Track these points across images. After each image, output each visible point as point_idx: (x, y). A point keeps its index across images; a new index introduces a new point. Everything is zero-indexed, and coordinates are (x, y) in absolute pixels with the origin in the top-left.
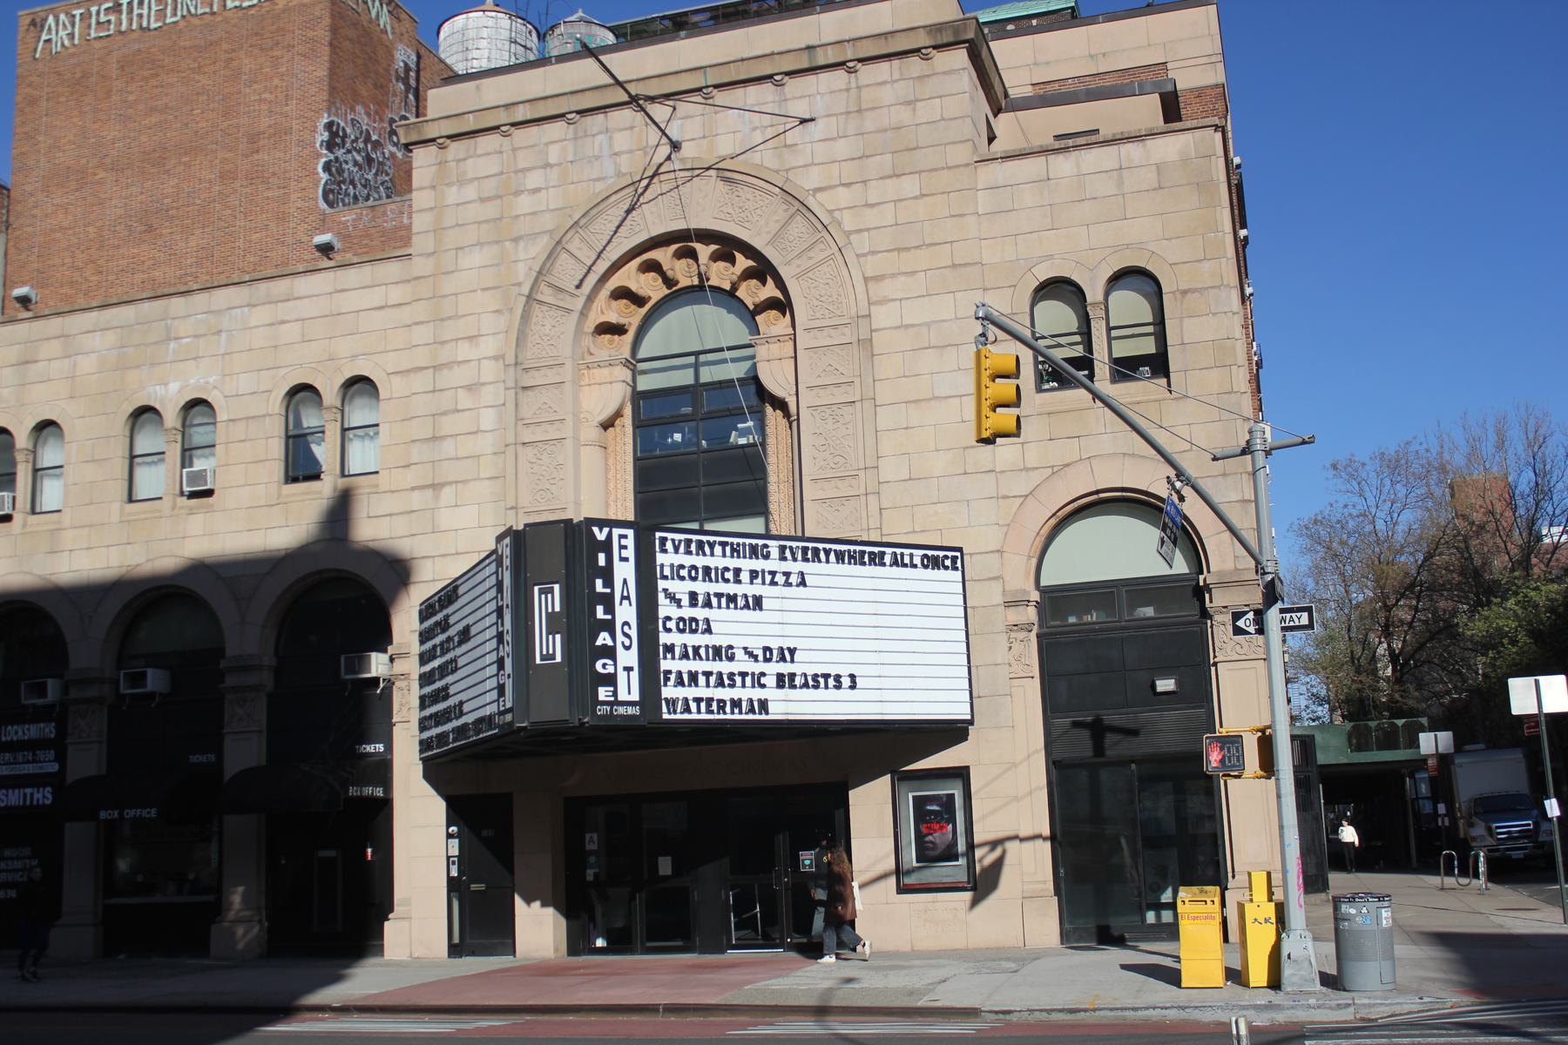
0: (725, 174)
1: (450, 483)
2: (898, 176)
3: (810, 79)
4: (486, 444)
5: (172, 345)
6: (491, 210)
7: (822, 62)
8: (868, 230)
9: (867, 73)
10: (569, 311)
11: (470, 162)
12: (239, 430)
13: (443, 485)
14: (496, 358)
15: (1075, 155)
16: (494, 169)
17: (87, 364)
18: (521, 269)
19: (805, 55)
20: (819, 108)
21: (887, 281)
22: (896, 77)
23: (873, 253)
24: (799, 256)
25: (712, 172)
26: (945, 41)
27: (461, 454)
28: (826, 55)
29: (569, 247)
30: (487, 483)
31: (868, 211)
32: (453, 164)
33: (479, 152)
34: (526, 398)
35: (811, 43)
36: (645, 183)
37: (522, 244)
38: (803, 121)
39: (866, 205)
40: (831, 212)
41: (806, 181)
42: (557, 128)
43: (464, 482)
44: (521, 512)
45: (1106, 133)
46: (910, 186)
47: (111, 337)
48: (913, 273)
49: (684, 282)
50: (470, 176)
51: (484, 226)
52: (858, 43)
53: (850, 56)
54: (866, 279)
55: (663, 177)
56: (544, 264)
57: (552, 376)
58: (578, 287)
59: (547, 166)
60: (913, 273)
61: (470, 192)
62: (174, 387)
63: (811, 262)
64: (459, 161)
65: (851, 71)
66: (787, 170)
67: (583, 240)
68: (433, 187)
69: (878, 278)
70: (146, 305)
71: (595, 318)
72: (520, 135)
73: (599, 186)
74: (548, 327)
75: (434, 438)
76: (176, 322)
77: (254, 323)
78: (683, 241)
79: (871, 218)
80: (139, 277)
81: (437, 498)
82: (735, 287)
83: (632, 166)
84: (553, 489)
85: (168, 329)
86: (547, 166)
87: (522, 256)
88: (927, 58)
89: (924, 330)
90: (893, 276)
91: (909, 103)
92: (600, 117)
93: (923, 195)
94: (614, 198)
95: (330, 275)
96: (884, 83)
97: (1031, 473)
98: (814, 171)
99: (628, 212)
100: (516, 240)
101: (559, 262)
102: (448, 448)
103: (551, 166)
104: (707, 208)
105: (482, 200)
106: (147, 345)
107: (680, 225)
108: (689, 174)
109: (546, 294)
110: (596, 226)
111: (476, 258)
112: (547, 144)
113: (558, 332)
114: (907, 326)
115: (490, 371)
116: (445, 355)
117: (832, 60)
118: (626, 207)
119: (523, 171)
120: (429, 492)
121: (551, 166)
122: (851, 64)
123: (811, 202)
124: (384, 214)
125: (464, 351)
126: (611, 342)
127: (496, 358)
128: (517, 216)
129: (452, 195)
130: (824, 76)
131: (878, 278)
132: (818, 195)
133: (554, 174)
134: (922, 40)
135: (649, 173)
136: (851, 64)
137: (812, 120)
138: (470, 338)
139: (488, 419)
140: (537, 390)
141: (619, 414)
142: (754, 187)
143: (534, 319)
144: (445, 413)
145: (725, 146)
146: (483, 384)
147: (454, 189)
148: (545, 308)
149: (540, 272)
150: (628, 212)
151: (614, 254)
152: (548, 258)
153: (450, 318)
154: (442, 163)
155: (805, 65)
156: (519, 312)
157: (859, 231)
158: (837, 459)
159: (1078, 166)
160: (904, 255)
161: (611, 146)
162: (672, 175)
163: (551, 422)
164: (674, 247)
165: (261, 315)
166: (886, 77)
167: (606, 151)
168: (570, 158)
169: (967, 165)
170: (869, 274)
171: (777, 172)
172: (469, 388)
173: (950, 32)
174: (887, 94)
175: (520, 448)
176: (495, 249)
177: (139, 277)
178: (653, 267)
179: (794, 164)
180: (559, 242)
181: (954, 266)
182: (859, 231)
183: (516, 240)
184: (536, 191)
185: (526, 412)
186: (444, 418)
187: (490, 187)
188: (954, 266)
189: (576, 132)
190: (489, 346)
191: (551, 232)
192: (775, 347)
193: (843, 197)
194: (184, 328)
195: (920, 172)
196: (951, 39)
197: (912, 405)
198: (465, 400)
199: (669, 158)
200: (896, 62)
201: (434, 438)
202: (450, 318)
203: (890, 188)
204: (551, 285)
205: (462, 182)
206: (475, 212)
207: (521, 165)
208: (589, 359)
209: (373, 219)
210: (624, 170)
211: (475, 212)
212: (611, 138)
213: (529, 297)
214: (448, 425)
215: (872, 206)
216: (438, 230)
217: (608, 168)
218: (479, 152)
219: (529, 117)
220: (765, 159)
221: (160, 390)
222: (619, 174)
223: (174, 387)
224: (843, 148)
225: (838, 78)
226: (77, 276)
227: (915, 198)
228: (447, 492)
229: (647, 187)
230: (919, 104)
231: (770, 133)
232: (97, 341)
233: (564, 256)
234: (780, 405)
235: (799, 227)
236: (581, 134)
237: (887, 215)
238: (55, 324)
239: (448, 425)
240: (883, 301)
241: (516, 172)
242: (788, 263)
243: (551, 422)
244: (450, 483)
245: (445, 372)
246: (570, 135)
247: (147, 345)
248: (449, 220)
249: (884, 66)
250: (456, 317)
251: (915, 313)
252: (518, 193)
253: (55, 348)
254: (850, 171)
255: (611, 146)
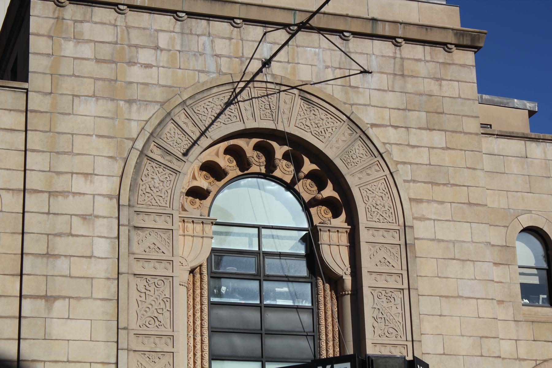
0: (305, 94)
1: (64, 298)
2: (431, 130)
3: (367, 43)
4: (101, 269)
6: (105, 71)
7: (380, 32)
8: (410, 164)
9: (409, 50)
10: (176, 172)
11: (86, 26)
13: (56, 298)
14: (110, 197)
15: (542, 145)
16: (111, 38)
18: (135, 128)
19: (370, 23)
20: (374, 64)
21: (425, 205)
22: (428, 58)
23: (414, 181)
24: (361, 171)
25: (295, 91)
26: (465, 43)
27: (74, 273)
28: (384, 29)
29: (176, 119)
30: (99, 302)
31: (410, 150)
32: (71, 23)
33: (95, 19)
34: (136, 236)
35: (376, 16)
36: (242, 85)
37: (135, 107)
38: (365, 72)
39: (408, 145)
40: (384, 144)
41: (366, 117)
42: (166, 21)
43: (78, 298)
44: (132, 333)
45: (496, 128)
46: (438, 139)
48: (442, 203)
49: (254, 169)
50: (86, 37)
51: (99, 83)
52: (407, 27)
53: (400, 34)
54: (411, 200)
55: (256, 84)
56: (155, 129)
57: (161, 223)
58: (185, 154)
59: (157, 48)
60: (442, 203)
61: (87, 51)
63: (370, 178)
64: (75, 21)
65: (397, 45)
66: (352, 105)
67: (188, 116)
68: (51, 37)
69: (419, 201)
71: (186, 183)
72: (134, 18)
73: (203, 78)
74: (157, 180)
75: (47, 255)
78: (265, 138)
79: (411, 155)
81: (50, 309)
82: (294, 181)
83: (231, 68)
84: (160, 317)
86: (157, 48)
87: (134, 116)
88: (449, 51)
89: (451, 245)
90: (428, 201)
91: (437, 79)
92: (204, 23)
93: (448, 148)
94: (215, 90)
96: (419, 60)
97: (522, 362)
98: (372, 111)
99: (228, 104)
100: (130, 102)
101: (167, 129)
102: (62, 266)
103: (162, 50)
104: (294, 119)
105: (98, 61)
107: (270, 125)
108: (278, 87)
109: (157, 154)
110: (200, 108)
111: (90, 108)
112: (157, 31)
113: (168, 186)
114: (439, 241)
115: (105, 207)
116: (60, 183)
117: (387, 33)
118: (226, 100)
119: (136, 46)
120: (41, 303)
121: (162, 50)
122: (399, 40)
123: (371, 132)
125: (79, 184)
126: (192, 203)
127: (110, 197)
128: (131, 83)
129: (69, 49)
130: (377, 43)
131: (419, 201)
132: (374, 129)
133: (164, 57)
134: (450, 38)
135: (247, 78)
136: (399, 40)
137: (371, 73)
138: (86, 175)
139: (102, 247)
140: (147, 232)
141: (201, 266)
142: (327, 111)
143: (146, 172)
144: (60, 235)
145: (305, 74)
146: (97, 217)
147: (71, 44)
148: (154, 165)
149: (151, 134)
150: (228, 104)
151: (216, 133)
152: (159, 124)
153: (65, 153)
154: (59, 19)
155: (369, 31)
156: (132, 162)
157: (404, 163)
158: (391, 330)
159: (545, 153)
160: (435, 187)
161: (213, 48)
162: (264, 85)
163: (160, 261)
164: (255, 141)
166: (421, 56)
167: (208, 51)
168: (178, 47)
169: (477, 134)
170: (413, 196)
171: (345, 103)
172: (84, 217)
173: (469, 38)
174: (422, 69)
175: (131, 278)
176: (110, 105)
178: (269, 153)
179: (356, 101)
180: (169, 114)
181: (470, 204)
182: (404, 163)
183: (130, 102)
184: (148, 66)
185: (137, 249)
186: (58, 239)
187: (106, 51)
188: (470, 204)
189: (182, 28)
190: (106, 185)
191: (162, 104)
192: (334, 235)
193: (392, 135)
195: (446, 131)
196: (469, 43)
197: (444, 299)
198: (78, 227)
199: (260, 71)
200: (428, 48)
201: (47, 255)
202: (65, 153)
203: (426, 137)
204: (160, 147)
205: (78, 40)
206: (89, 67)
207: (134, 42)
208: (184, 214)
210: (224, 70)
211: (89, 67)
212: (212, 41)
213: (142, 152)
214: (62, 245)
215: (414, 147)
216: (55, 75)
217: (211, 65)
218: (95, 19)
219: (146, 5)
220: (334, 91)
222: (220, 72)
224: (392, 99)
225: (386, 47)
227: (442, 149)
228: (59, 305)
229: (243, 89)
230: (444, 83)
231: (339, 73)
233: (171, 126)
234: (335, 282)
235: (359, 148)
236: (188, 31)
237: (423, 157)
239: (62, 245)
240: (422, 219)
241: (130, 46)
242: (353, 175)
243: (160, 261)
244: (64, 298)
245: (60, 198)
246: (177, 29)
248: (66, 68)
249: (419, 48)
250: (71, 153)
251: (446, 232)
252: (131, 63)
254: (396, 117)
255: (213, 48)
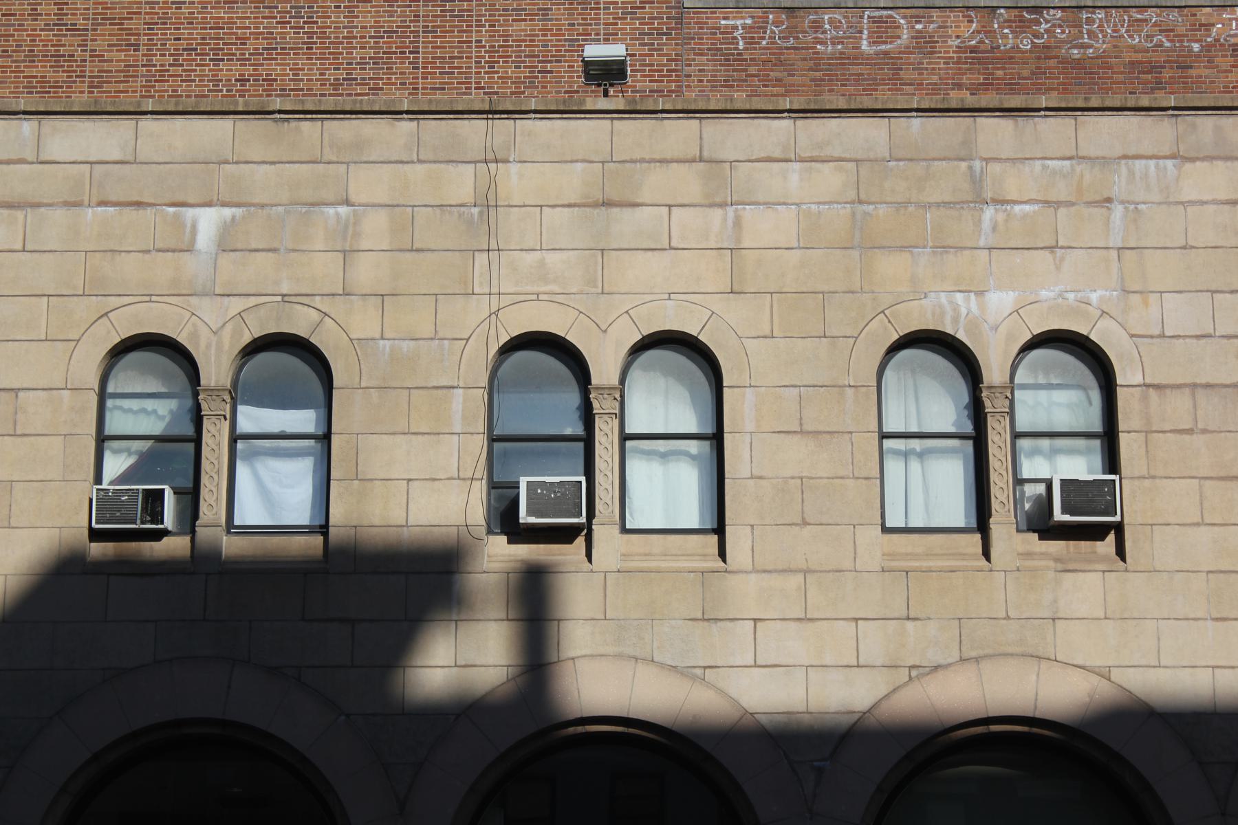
5: (989, 213)
12: (1178, 408)
17: (766, 228)
47: (830, 180)
62: (1001, 301)
70: (916, 124)
76: (995, 168)
77: (1189, 194)
80: (230, 70)
85: (976, 181)
95: (604, 124)
106: (927, 206)
124: (817, 26)
165: (1206, 181)
177: (230, 70)
194: (1014, 182)
209: (792, 32)
221: (966, 304)
223: (1001, 301)
226: (70, 43)
232: (793, 179)
238: (679, 134)
247: (927, 206)
253: (688, 182)
